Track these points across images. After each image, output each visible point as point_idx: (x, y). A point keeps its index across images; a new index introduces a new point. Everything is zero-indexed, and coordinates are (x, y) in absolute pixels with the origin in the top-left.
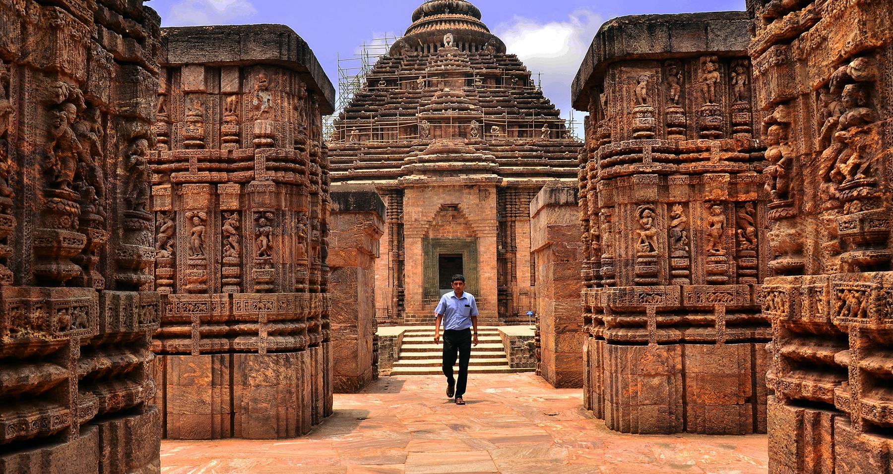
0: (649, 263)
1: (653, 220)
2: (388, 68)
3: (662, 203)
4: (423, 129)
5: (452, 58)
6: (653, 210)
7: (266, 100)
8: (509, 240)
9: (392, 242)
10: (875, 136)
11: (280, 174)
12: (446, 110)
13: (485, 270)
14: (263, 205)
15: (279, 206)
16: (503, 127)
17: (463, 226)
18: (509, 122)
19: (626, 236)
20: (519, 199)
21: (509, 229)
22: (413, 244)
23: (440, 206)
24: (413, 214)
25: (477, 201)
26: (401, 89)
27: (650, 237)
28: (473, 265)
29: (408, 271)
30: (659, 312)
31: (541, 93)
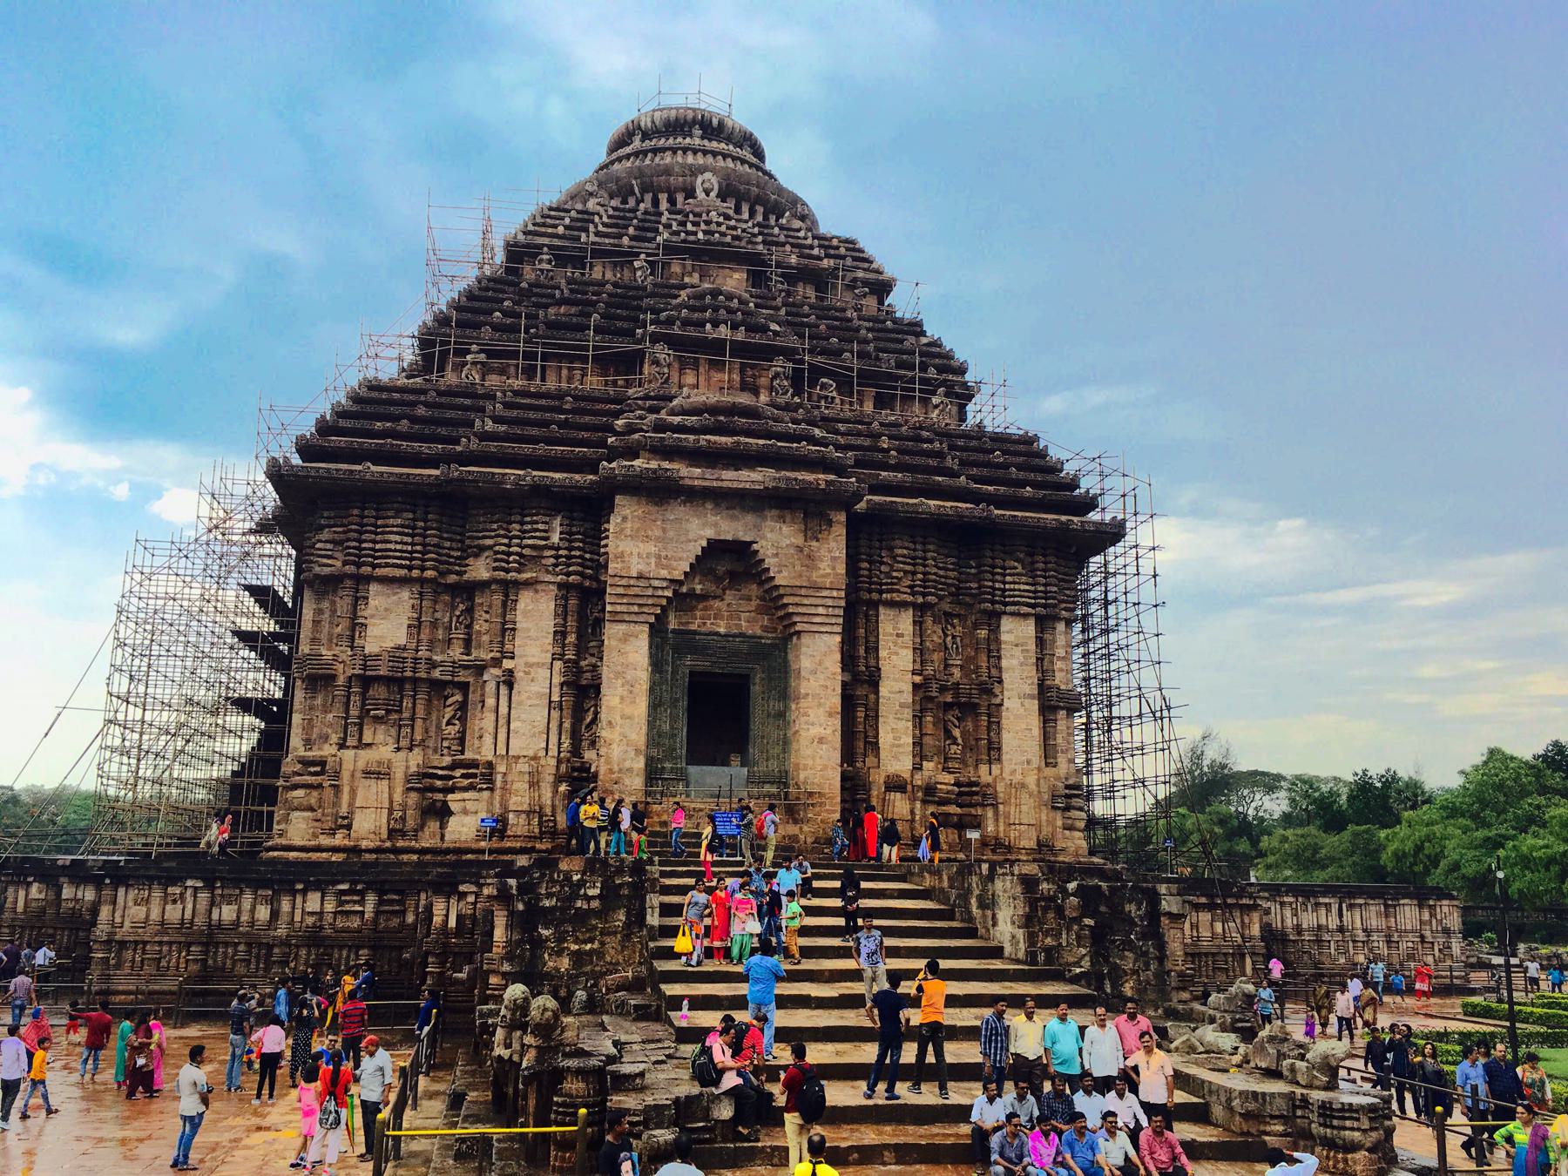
4: (656, 362)
5: (721, 219)
8: (862, 652)
9: (564, 634)
12: (716, 325)
13: (812, 719)
16: (845, 386)
17: (754, 603)
20: (891, 549)
21: (861, 621)
22: (625, 639)
23: (704, 544)
24: (635, 560)
25: (799, 540)
28: (779, 706)
29: (611, 709)
31: (919, 324)
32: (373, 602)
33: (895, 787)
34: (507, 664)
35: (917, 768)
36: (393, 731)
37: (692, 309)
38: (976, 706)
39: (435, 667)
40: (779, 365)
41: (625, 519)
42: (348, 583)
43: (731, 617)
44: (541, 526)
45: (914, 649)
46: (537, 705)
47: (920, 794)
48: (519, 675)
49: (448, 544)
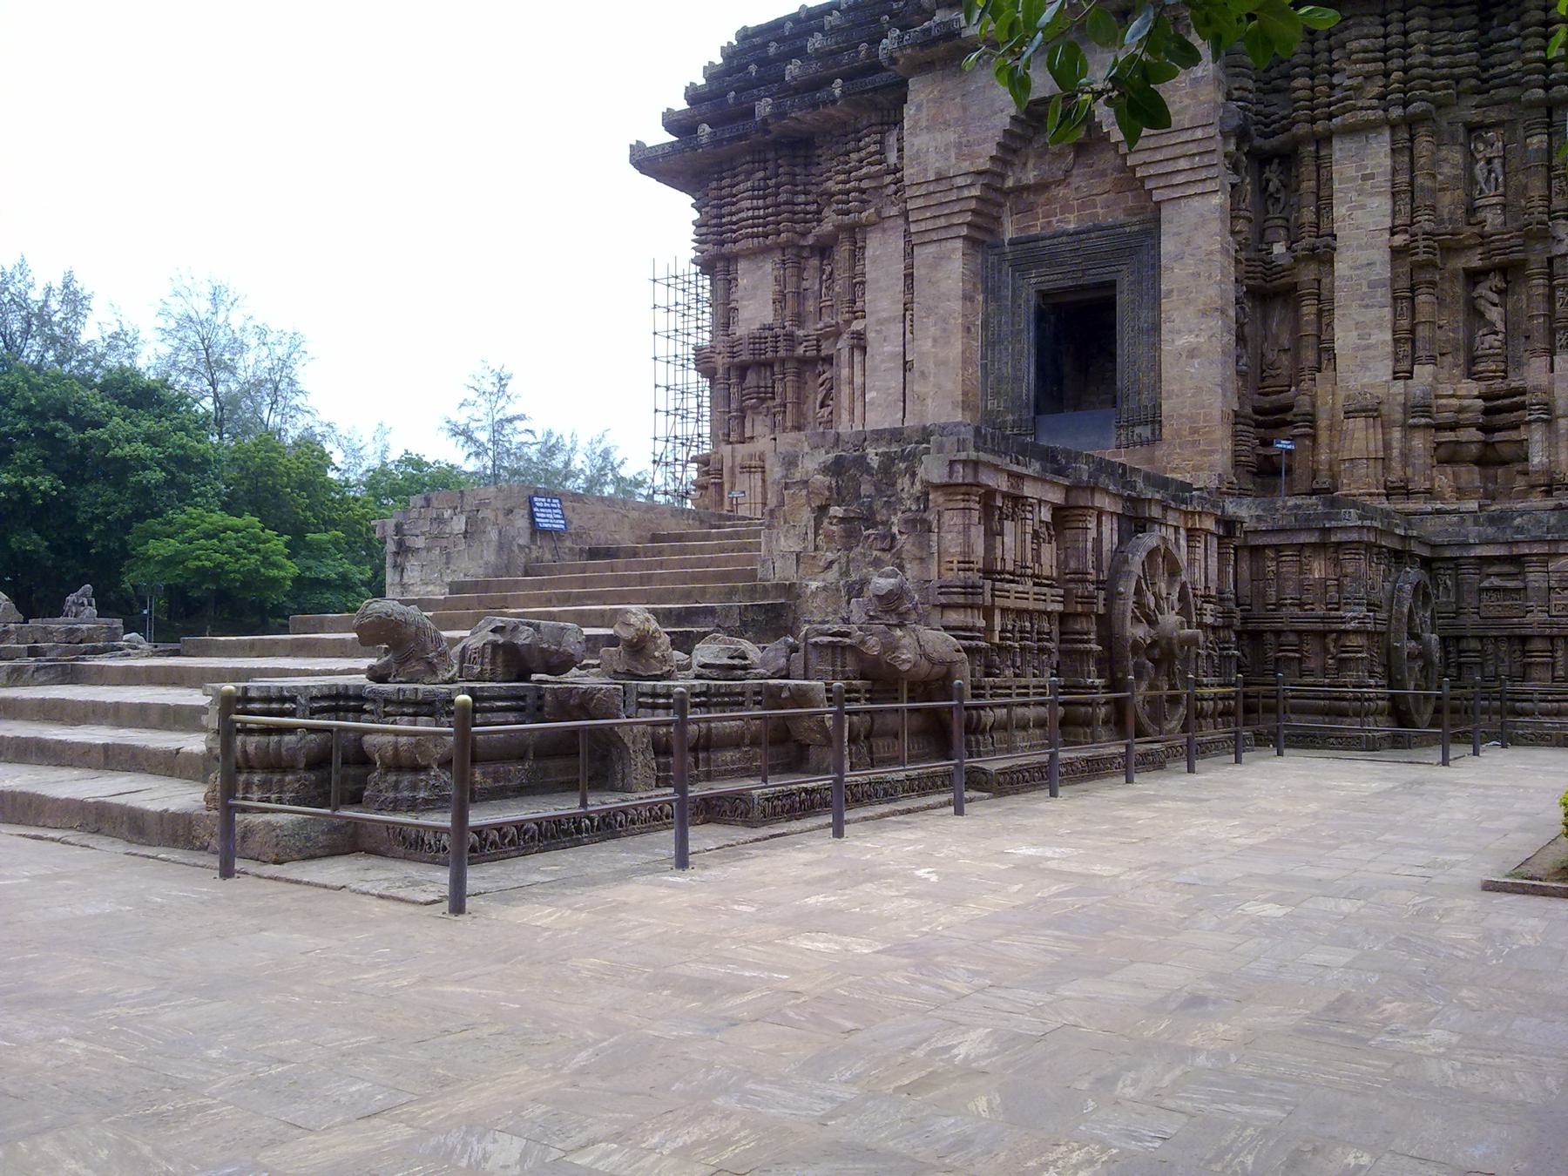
8: (1308, 215)
13: (1178, 324)
17: (1109, 179)
20: (1343, 46)
21: (1307, 169)
24: (932, 157)
32: (742, 282)
33: (1356, 411)
34: (857, 326)
35: (1402, 375)
36: (768, 421)
38: (1523, 264)
39: (801, 344)
41: (919, 107)
42: (720, 265)
43: (1083, 206)
44: (873, 148)
45: (1393, 194)
46: (891, 369)
47: (1398, 415)
48: (871, 335)
49: (802, 198)
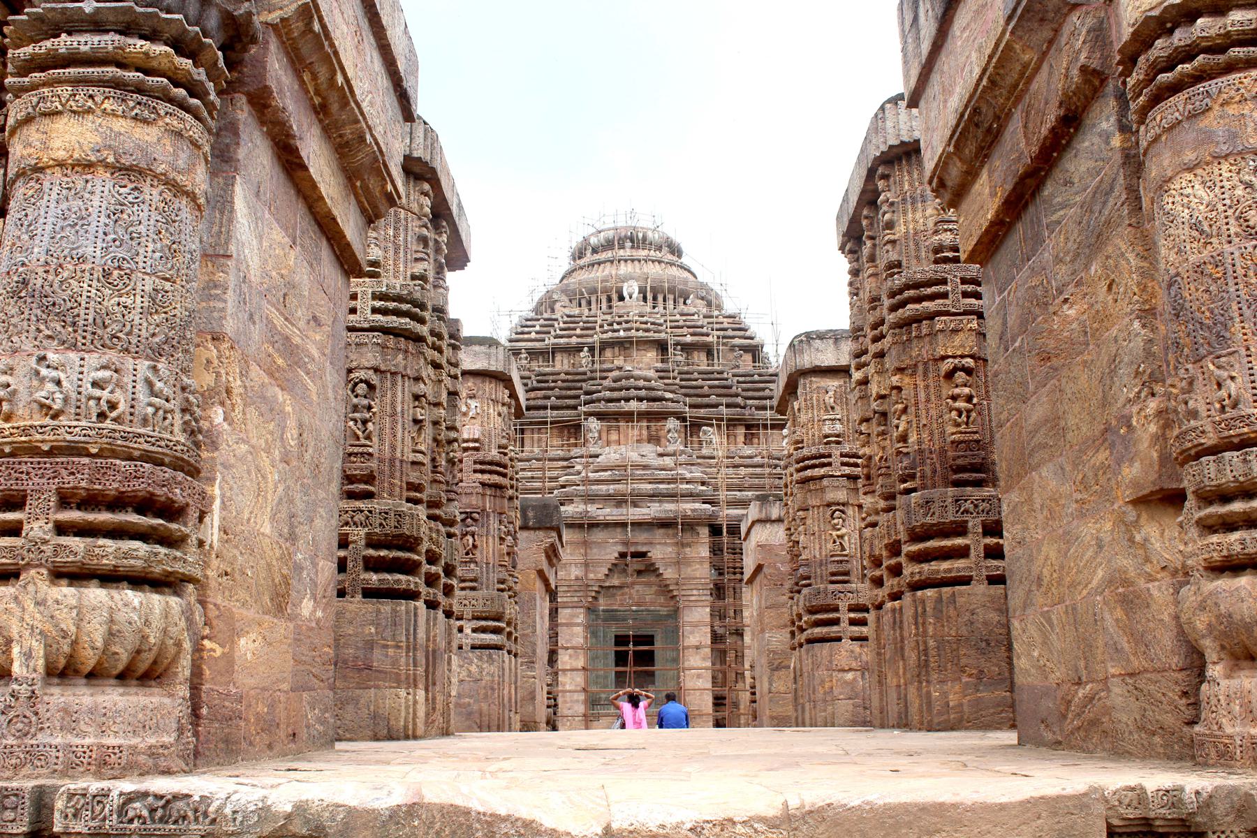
0: (841, 562)
1: (844, 521)
2: (533, 334)
3: (852, 505)
6: (843, 512)
7: (473, 407)
10: (888, 442)
11: (486, 477)
14: (470, 506)
15: (484, 506)
18: (729, 420)
19: (820, 536)
23: (617, 555)
26: (554, 366)
27: (841, 537)
30: (851, 609)
37: (612, 390)
40: (672, 423)
